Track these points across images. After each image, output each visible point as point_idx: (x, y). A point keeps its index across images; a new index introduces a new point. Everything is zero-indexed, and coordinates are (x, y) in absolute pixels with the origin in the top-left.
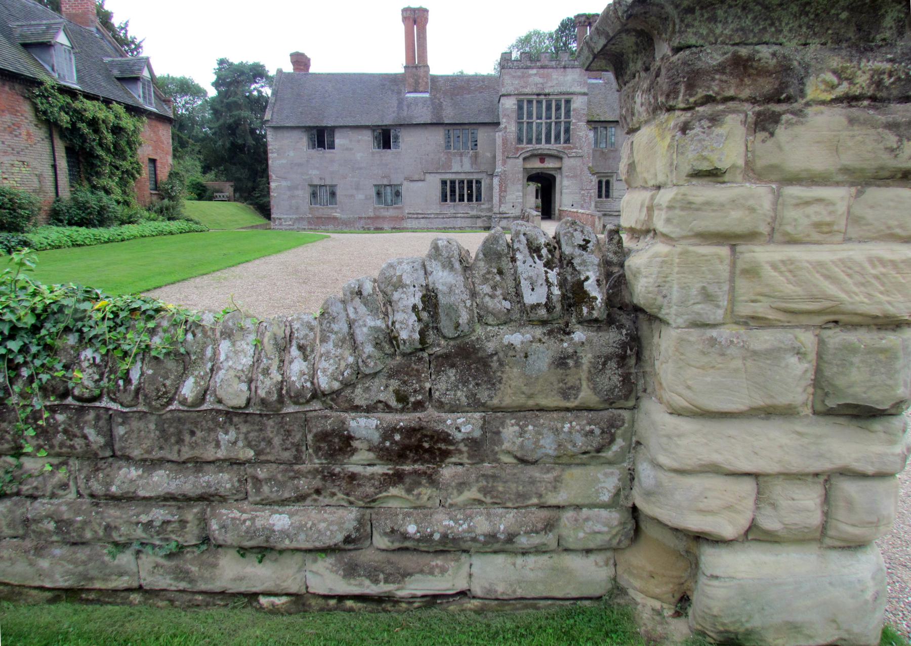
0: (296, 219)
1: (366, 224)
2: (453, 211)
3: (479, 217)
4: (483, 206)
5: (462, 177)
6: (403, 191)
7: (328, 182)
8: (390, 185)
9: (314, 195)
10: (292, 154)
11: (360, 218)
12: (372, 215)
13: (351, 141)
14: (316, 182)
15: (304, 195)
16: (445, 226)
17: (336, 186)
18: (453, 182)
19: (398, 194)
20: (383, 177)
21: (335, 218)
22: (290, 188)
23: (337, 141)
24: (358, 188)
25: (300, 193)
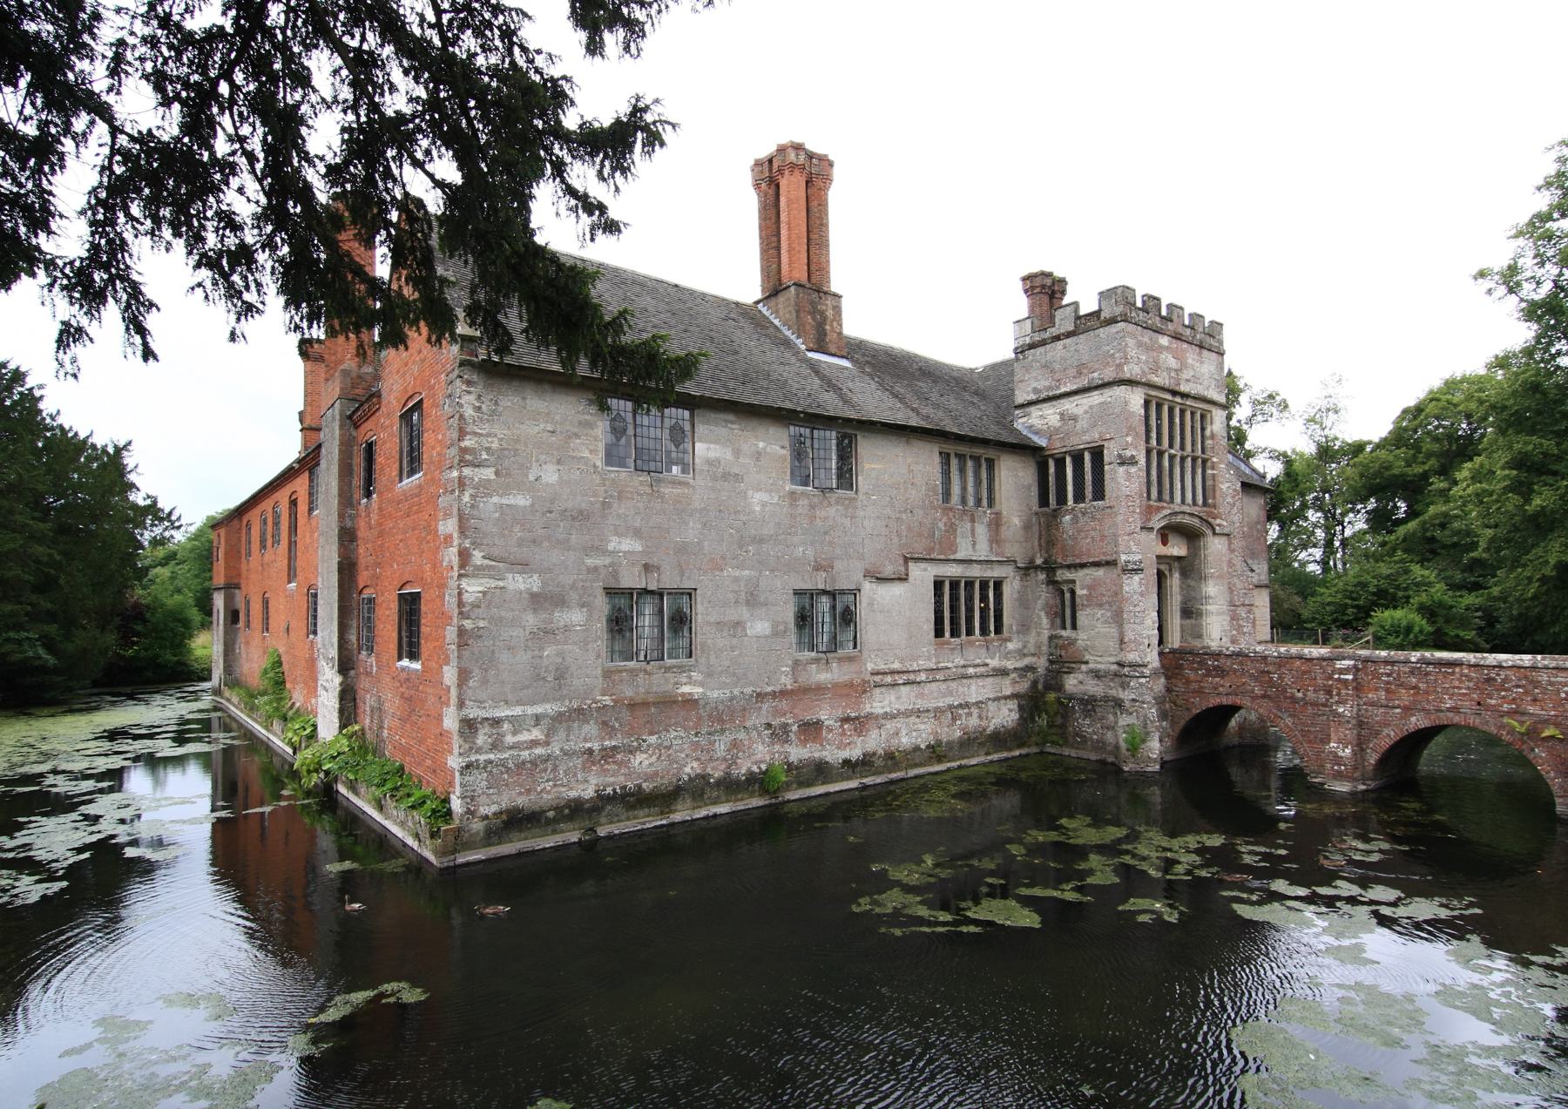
0: (559, 718)
1: (777, 712)
2: (959, 661)
3: (1003, 673)
4: (1010, 646)
5: (975, 572)
6: (863, 612)
7: (669, 579)
8: (832, 595)
9: (619, 624)
10: (550, 475)
11: (760, 696)
12: (786, 681)
13: (737, 453)
14: (631, 579)
15: (584, 621)
16: (950, 700)
17: (690, 594)
18: (954, 585)
19: (847, 618)
20: (817, 568)
21: (690, 703)
22: (537, 600)
23: (704, 450)
24: (752, 600)
25: (576, 617)
